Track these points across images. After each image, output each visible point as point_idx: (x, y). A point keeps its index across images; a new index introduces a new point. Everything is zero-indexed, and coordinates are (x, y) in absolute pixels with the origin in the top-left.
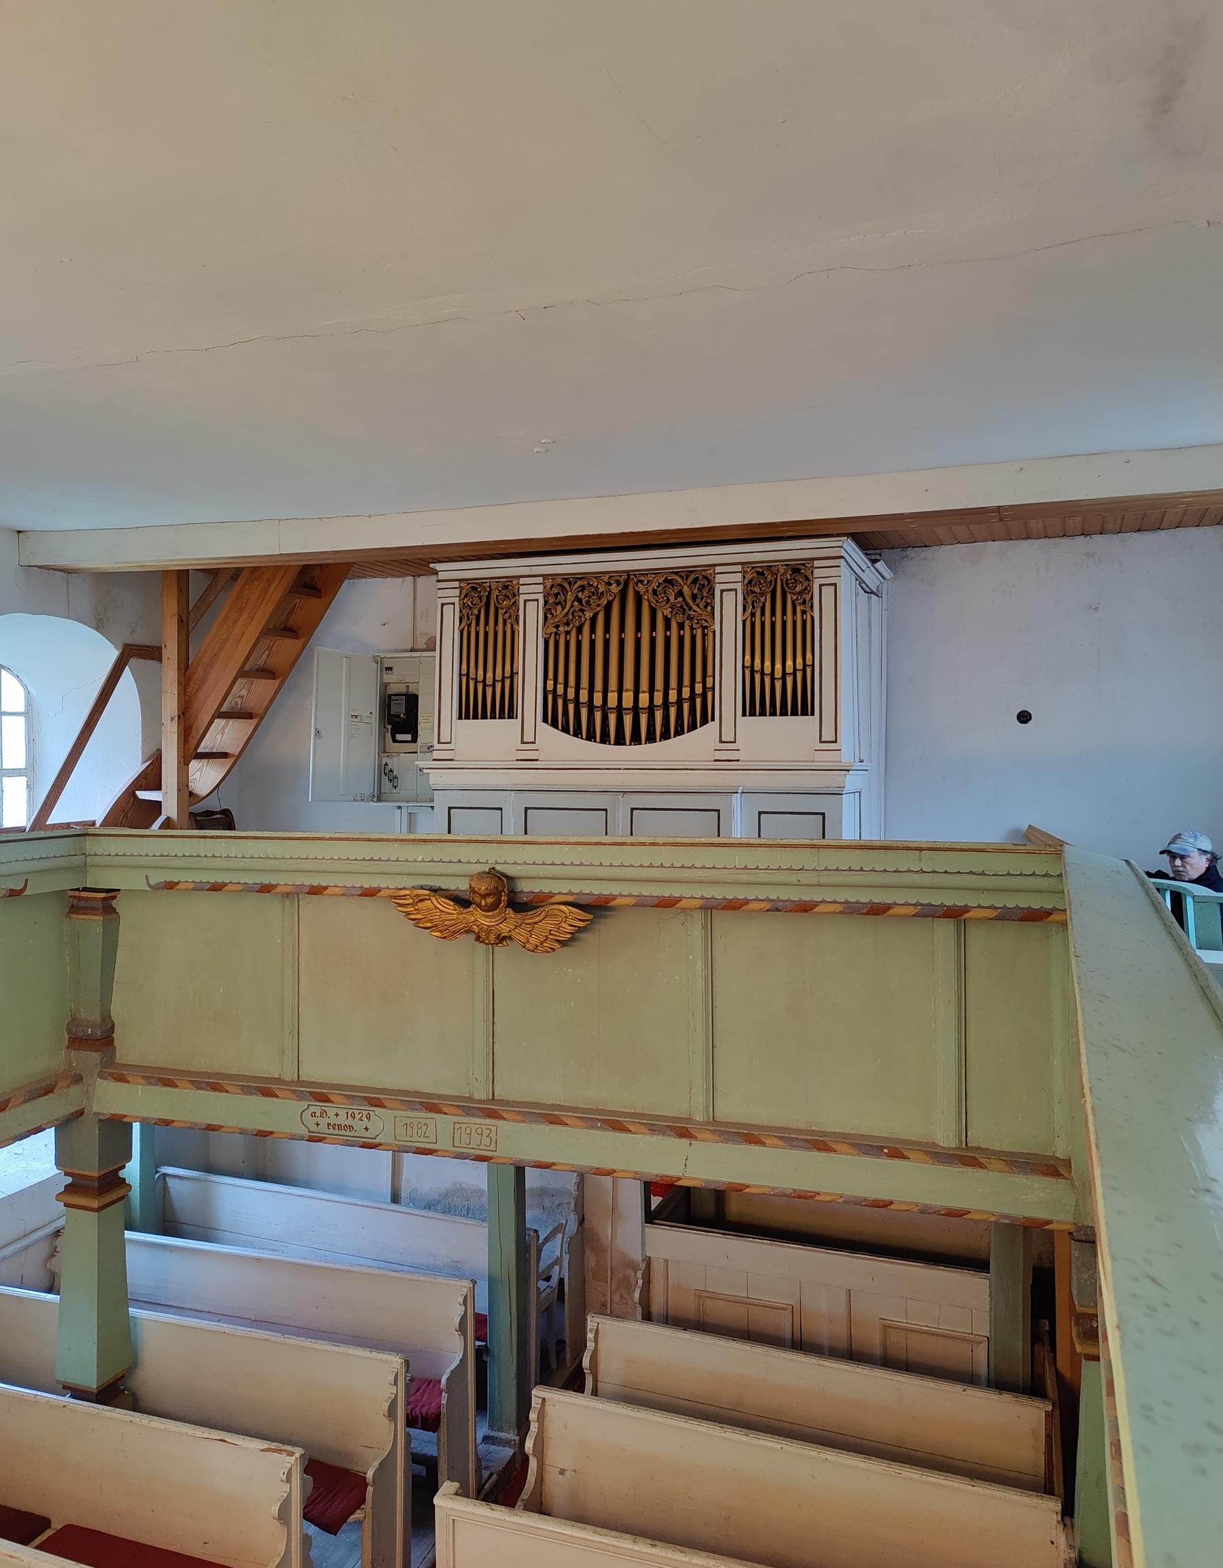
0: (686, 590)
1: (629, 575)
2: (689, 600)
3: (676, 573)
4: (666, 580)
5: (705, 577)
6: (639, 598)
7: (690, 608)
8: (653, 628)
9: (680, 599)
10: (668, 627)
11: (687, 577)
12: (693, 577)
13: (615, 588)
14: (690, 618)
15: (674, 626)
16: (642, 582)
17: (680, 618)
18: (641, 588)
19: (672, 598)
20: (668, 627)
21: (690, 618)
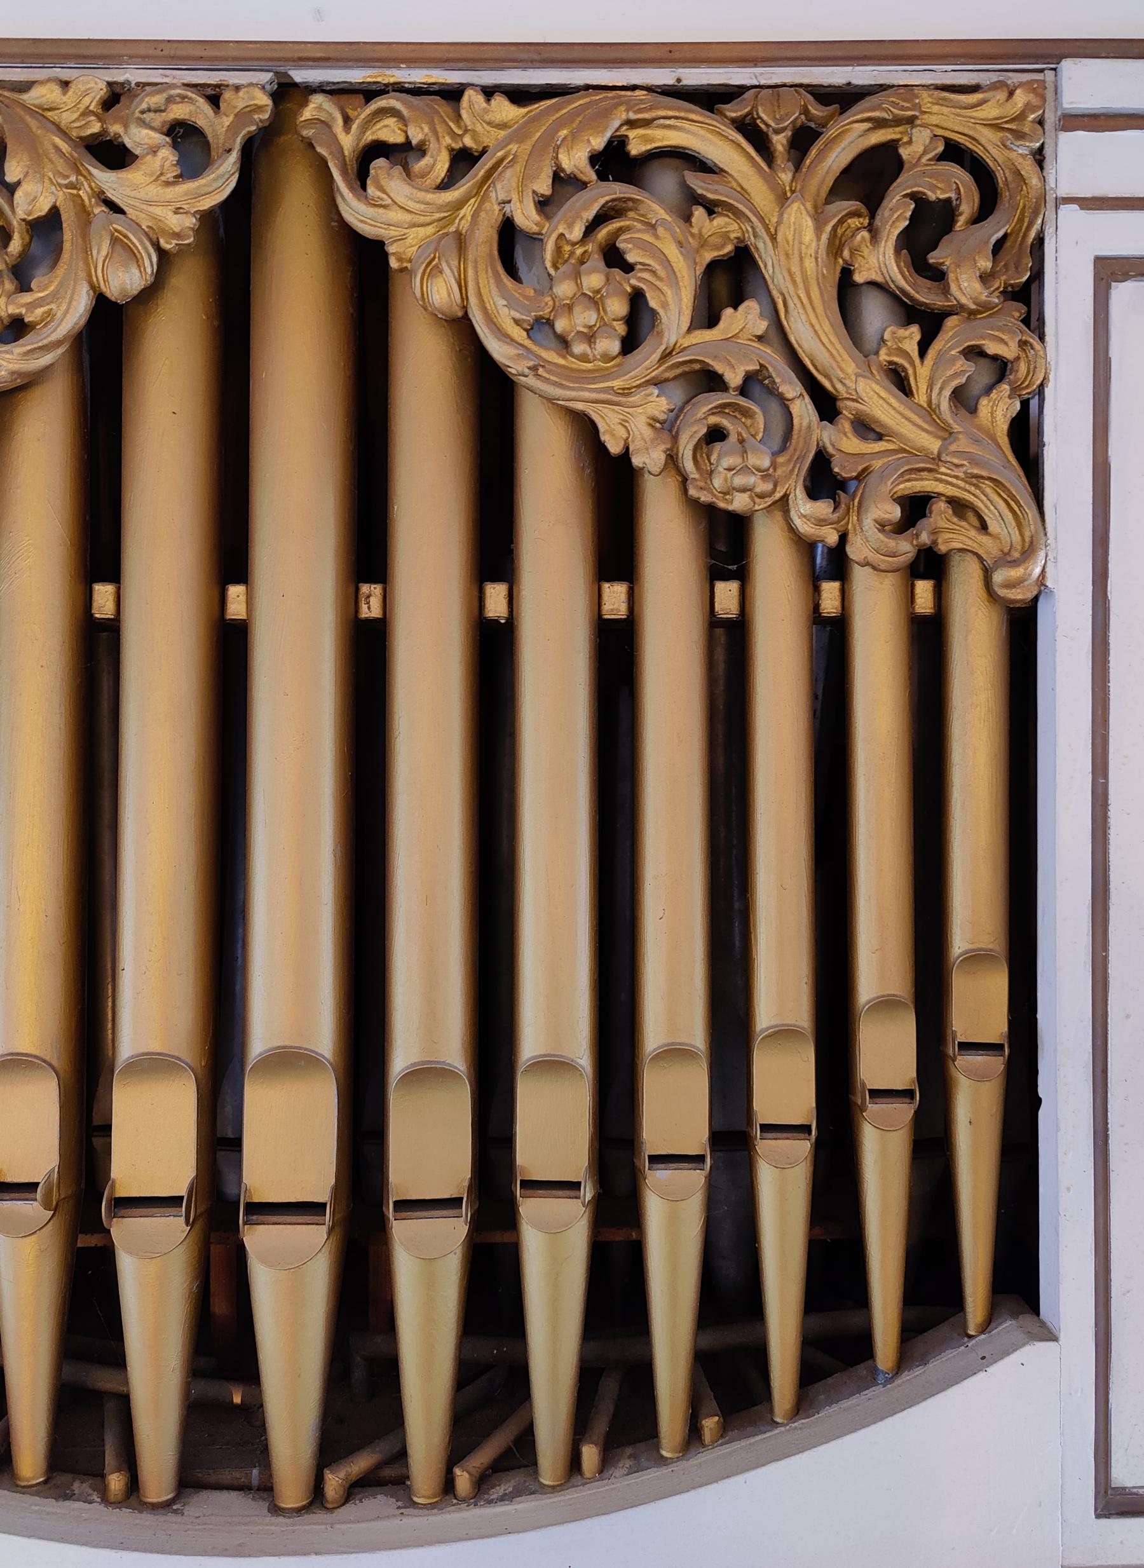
0: (796, 246)
1: (287, 93)
2: (815, 332)
3: (709, 99)
4: (614, 161)
5: (954, 152)
6: (366, 276)
7: (827, 406)
8: (493, 548)
9: (744, 320)
10: (615, 550)
11: (804, 139)
12: (848, 140)
13: (164, 200)
14: (823, 480)
15: (667, 542)
16: (402, 153)
17: (738, 478)
18: (397, 212)
19: (674, 307)
20: (615, 550)
21: (823, 480)
